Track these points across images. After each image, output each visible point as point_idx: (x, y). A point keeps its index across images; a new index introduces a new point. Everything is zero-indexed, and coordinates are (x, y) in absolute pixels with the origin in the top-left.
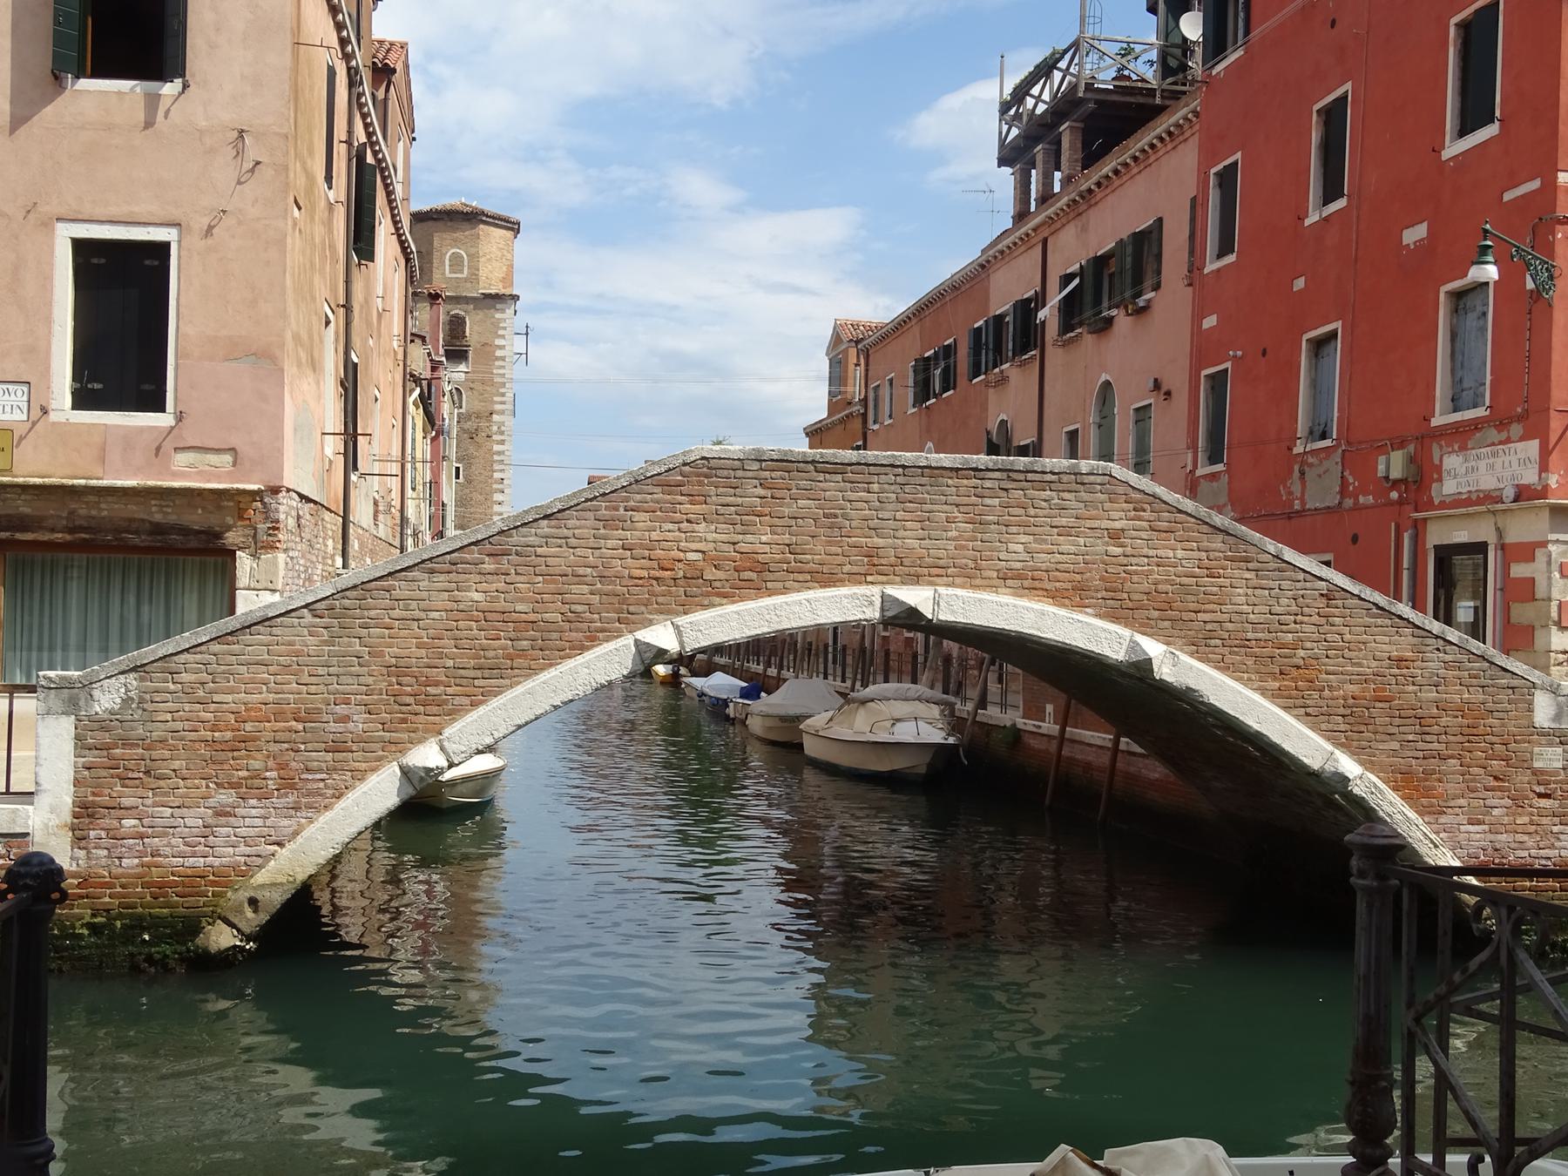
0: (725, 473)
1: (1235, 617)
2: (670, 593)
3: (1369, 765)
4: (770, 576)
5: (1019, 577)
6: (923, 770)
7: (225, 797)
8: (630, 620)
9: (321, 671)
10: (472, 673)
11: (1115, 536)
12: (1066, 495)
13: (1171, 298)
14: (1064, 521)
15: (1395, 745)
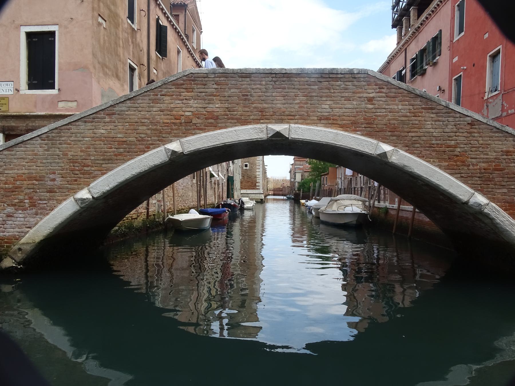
0: (201, 79)
1: (426, 134)
2: (178, 129)
3: (492, 199)
4: (219, 121)
5: (327, 119)
6: (355, 223)
7: (10, 210)
8: (164, 141)
9: (44, 161)
10: (101, 162)
11: (370, 100)
12: (347, 83)
13: (444, 59)
14: (347, 95)
15: (505, 190)
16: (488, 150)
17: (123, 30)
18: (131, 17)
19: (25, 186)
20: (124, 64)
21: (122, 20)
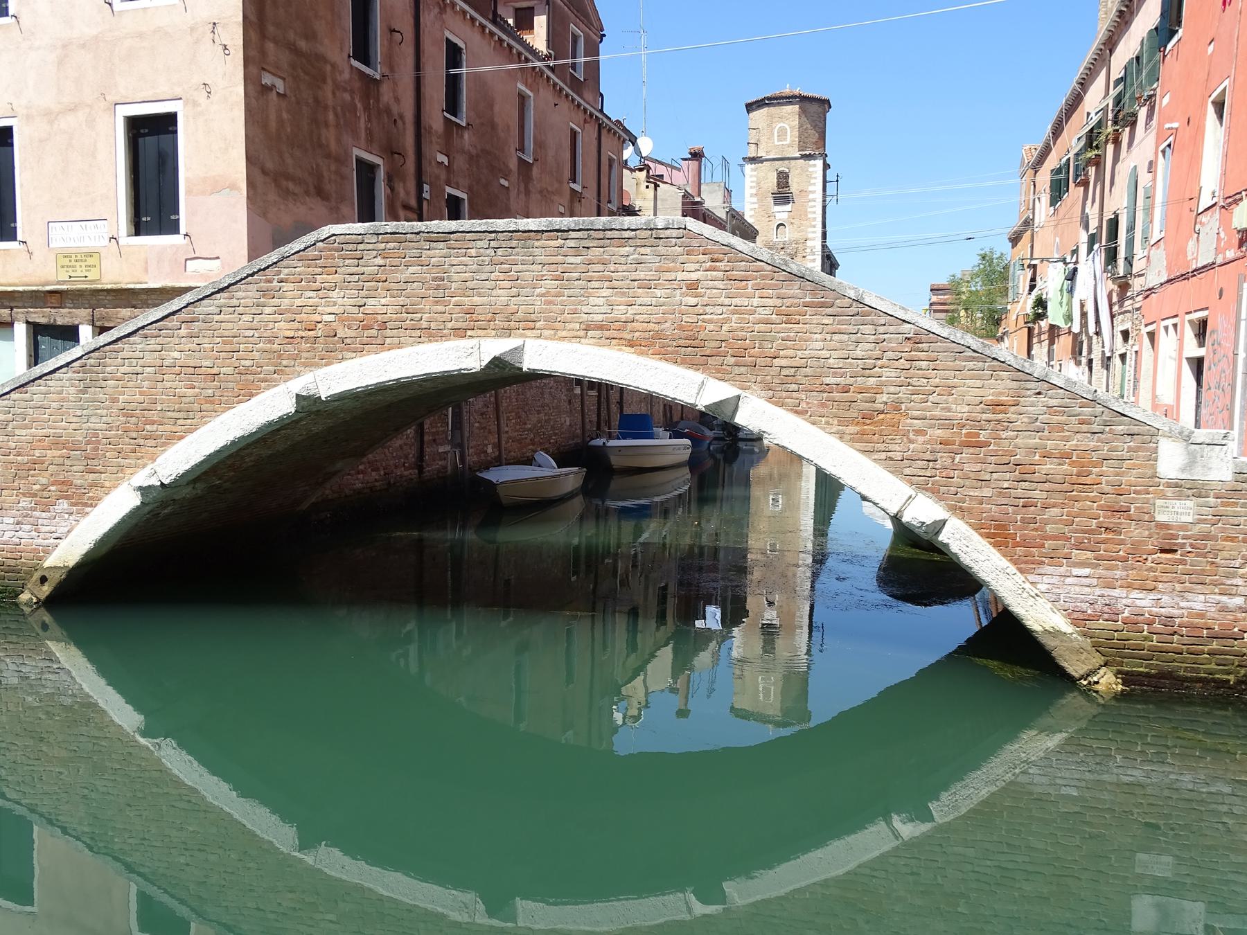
0: (351, 247)
5: (601, 328)
11: (693, 286)
12: (642, 250)
14: (642, 275)
15: (987, 492)
16: (951, 399)
17: (337, 87)
18: (362, 51)
19: (48, 459)
20: (342, 160)
21: (334, 66)
